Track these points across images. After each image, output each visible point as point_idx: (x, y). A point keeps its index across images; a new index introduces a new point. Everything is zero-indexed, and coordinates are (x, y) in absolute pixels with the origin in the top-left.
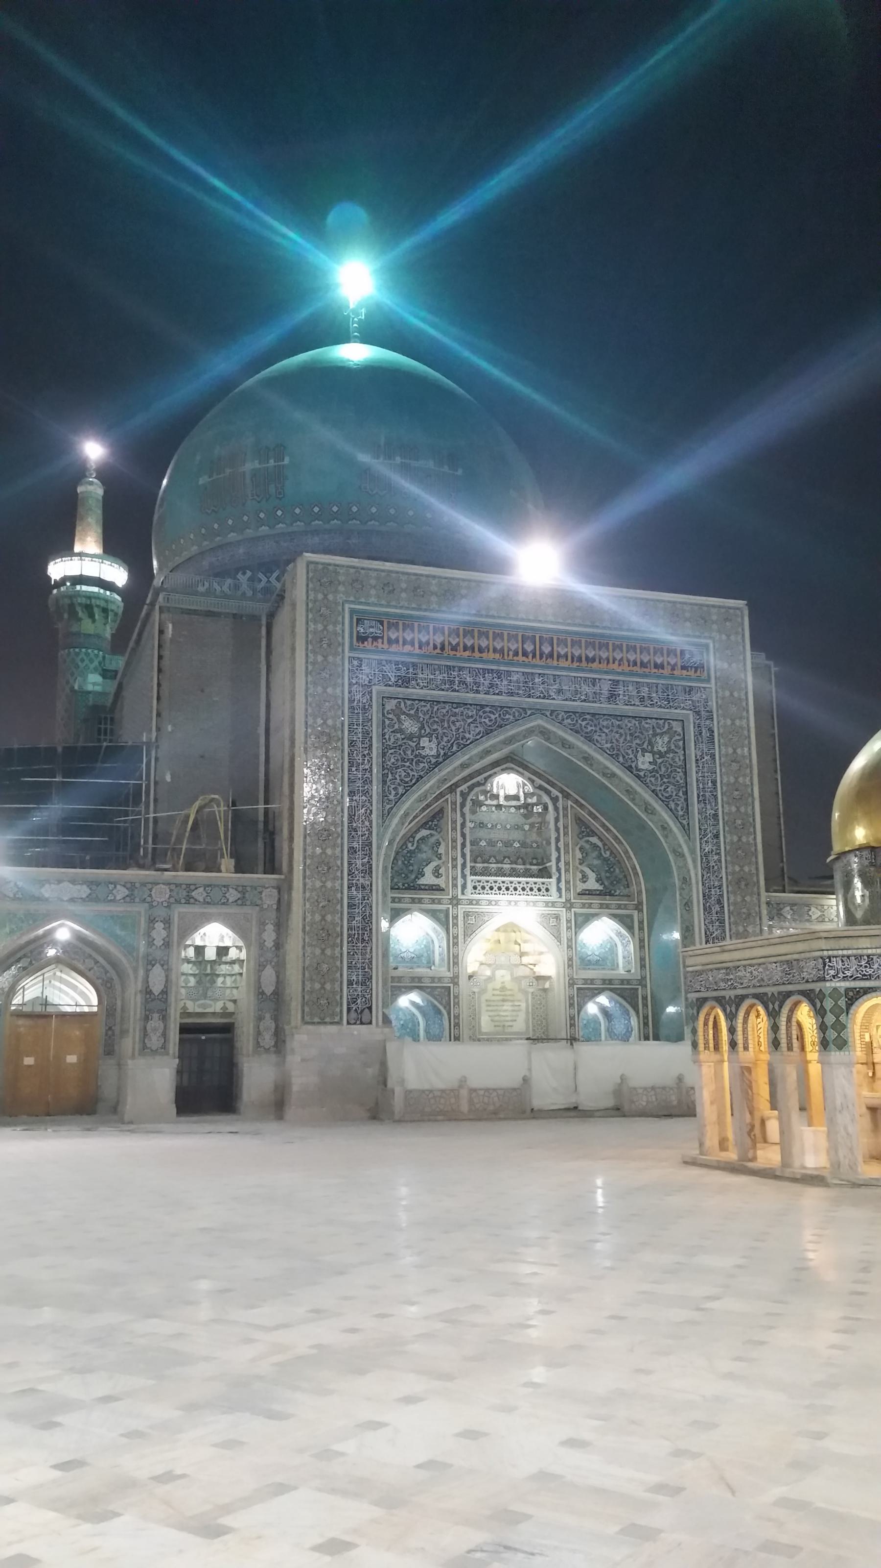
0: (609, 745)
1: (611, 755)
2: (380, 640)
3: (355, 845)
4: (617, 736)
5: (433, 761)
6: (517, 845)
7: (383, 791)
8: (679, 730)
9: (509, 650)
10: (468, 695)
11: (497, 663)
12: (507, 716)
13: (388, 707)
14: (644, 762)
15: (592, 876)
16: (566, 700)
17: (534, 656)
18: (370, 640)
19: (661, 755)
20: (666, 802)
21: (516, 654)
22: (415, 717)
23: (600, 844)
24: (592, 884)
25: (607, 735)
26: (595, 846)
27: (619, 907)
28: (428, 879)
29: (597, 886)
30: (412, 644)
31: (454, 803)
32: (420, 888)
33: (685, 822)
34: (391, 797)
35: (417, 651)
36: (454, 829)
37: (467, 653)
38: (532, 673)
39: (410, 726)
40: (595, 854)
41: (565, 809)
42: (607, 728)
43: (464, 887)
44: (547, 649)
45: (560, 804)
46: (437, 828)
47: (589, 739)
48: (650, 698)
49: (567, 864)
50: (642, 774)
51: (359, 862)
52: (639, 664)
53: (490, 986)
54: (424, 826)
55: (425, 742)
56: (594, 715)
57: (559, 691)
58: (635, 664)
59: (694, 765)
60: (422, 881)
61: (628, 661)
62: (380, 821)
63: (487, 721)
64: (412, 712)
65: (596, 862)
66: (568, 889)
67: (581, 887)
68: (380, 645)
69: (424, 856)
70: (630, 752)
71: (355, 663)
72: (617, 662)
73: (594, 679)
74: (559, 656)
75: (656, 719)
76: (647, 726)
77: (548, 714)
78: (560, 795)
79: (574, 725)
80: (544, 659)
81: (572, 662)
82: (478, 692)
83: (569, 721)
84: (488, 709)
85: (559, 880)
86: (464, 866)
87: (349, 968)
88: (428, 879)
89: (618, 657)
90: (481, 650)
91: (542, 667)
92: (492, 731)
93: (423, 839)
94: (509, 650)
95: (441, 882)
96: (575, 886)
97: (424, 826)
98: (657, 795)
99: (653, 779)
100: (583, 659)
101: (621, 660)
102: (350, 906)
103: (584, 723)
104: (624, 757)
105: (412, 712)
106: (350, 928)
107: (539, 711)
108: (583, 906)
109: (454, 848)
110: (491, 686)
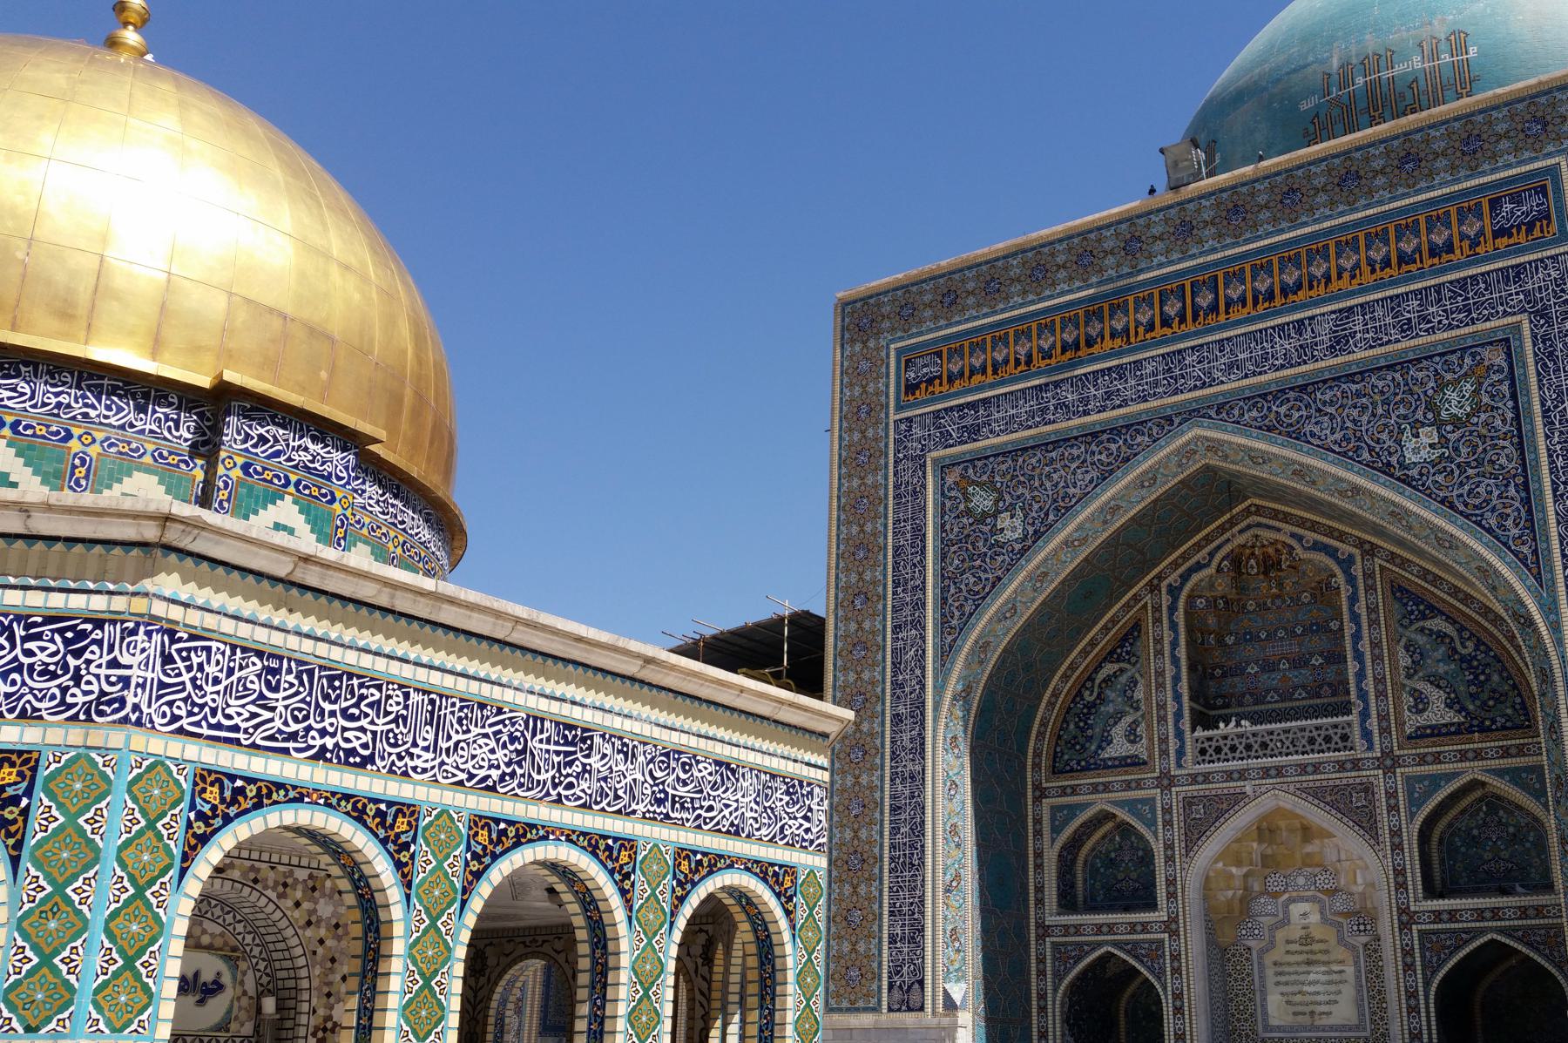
0: (1338, 436)
1: (1344, 454)
2: (937, 382)
3: (901, 709)
4: (1355, 413)
5: (1017, 547)
6: (1317, 661)
7: (943, 615)
9: (1138, 324)
10: (1071, 423)
11: (1120, 354)
12: (1139, 439)
13: (950, 480)
14: (1419, 447)
15: (1436, 697)
16: (1246, 376)
17: (1183, 320)
18: (923, 386)
19: (1456, 422)
20: (1474, 517)
21: (1151, 327)
22: (990, 486)
23: (1449, 629)
24: (1439, 712)
25: (1332, 417)
26: (1441, 636)
28: (1119, 747)
29: (1451, 717)
31: (1157, 609)
32: (1105, 766)
34: (954, 622)
35: (990, 379)
36: (1159, 653)
37: (1068, 355)
38: (1179, 352)
39: (982, 501)
41: (1369, 575)
42: (1331, 403)
43: (1180, 753)
44: (1205, 300)
45: (1357, 570)
46: (1132, 658)
47: (1296, 435)
48: (1425, 319)
49: (1380, 680)
50: (1414, 472)
51: (906, 737)
52: (1394, 260)
53: (1280, 935)
54: (1110, 656)
55: (1004, 521)
56: (1303, 388)
58: (1387, 263)
60: (1110, 752)
61: (1371, 263)
62: (938, 665)
63: (1103, 457)
64: (985, 478)
66: (1385, 731)
67: (1412, 722)
68: (937, 389)
69: (1110, 708)
70: (1384, 436)
71: (903, 427)
72: (1346, 275)
73: (1301, 322)
75: (1441, 355)
76: (1420, 375)
77: (1212, 413)
78: (1356, 552)
79: (1264, 417)
80: (1201, 319)
81: (1255, 303)
82: (1086, 413)
83: (1254, 413)
84: (1105, 437)
85: (1365, 715)
86: (1178, 715)
87: (892, 913)
88: (1119, 747)
89: (1348, 265)
90: (1089, 344)
91: (1197, 334)
92: (1111, 472)
93: (1107, 680)
95: (1140, 750)
96: (1401, 724)
97: (1110, 656)
98: (1452, 506)
99: (1440, 478)
100: (1277, 291)
101: (1357, 266)
102: (895, 810)
103: (1283, 410)
104: (1371, 449)
105: (985, 478)
106: (893, 847)
107: (1193, 413)
108: (1422, 760)
109: (1161, 686)
110: (1108, 395)
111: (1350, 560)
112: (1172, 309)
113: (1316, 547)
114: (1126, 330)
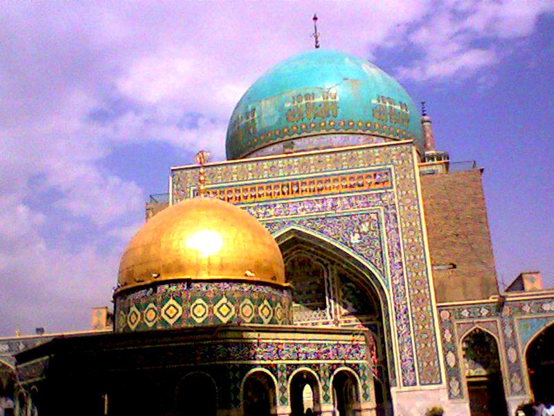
8: (375, 218)
9: (275, 193)
17: (288, 193)
19: (365, 234)
23: (354, 286)
26: (351, 287)
27: (367, 321)
30: (255, 196)
33: (381, 269)
40: (351, 292)
44: (295, 189)
45: (329, 268)
50: (353, 246)
57: (303, 210)
59: (385, 236)
65: (351, 297)
66: (336, 313)
74: (302, 191)
78: (329, 262)
90: (260, 196)
91: (292, 199)
94: (275, 193)
96: (340, 312)
110: (265, 213)
111: (327, 264)
112: (285, 190)
113: (318, 260)
114: (271, 194)
